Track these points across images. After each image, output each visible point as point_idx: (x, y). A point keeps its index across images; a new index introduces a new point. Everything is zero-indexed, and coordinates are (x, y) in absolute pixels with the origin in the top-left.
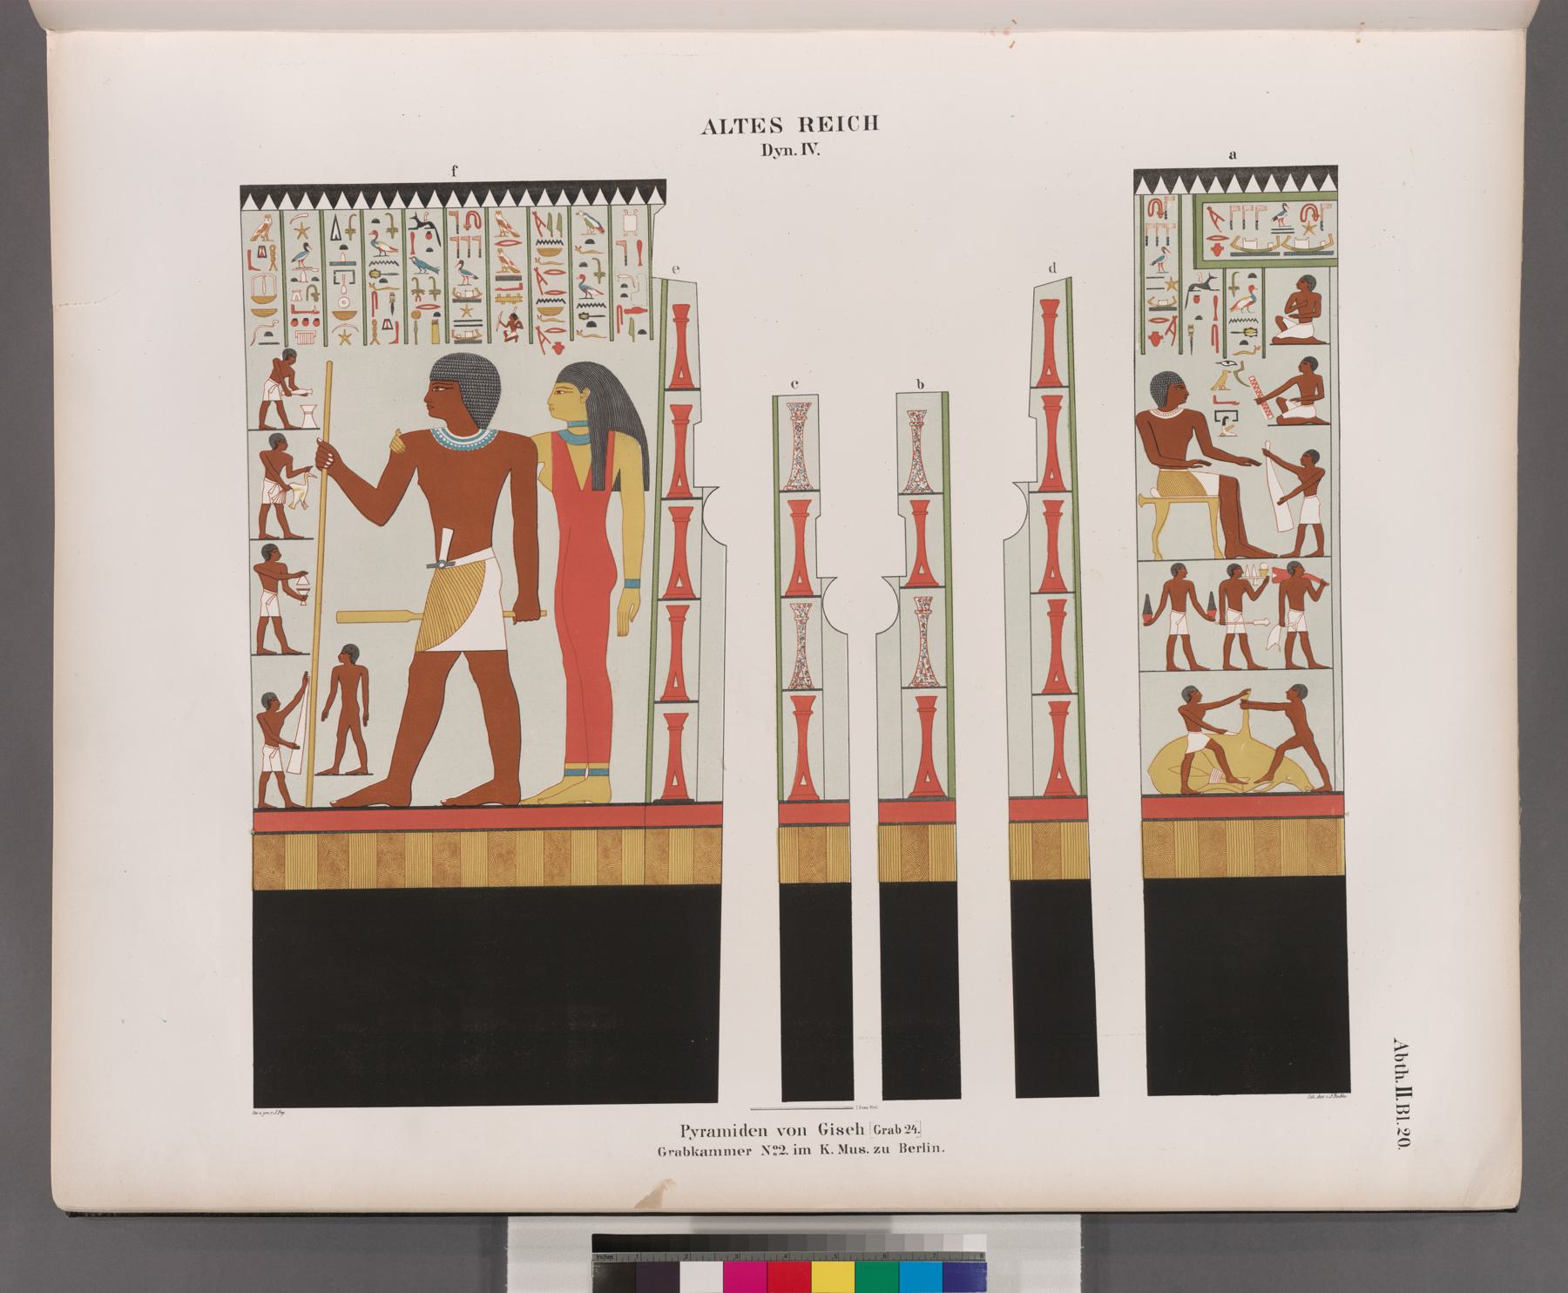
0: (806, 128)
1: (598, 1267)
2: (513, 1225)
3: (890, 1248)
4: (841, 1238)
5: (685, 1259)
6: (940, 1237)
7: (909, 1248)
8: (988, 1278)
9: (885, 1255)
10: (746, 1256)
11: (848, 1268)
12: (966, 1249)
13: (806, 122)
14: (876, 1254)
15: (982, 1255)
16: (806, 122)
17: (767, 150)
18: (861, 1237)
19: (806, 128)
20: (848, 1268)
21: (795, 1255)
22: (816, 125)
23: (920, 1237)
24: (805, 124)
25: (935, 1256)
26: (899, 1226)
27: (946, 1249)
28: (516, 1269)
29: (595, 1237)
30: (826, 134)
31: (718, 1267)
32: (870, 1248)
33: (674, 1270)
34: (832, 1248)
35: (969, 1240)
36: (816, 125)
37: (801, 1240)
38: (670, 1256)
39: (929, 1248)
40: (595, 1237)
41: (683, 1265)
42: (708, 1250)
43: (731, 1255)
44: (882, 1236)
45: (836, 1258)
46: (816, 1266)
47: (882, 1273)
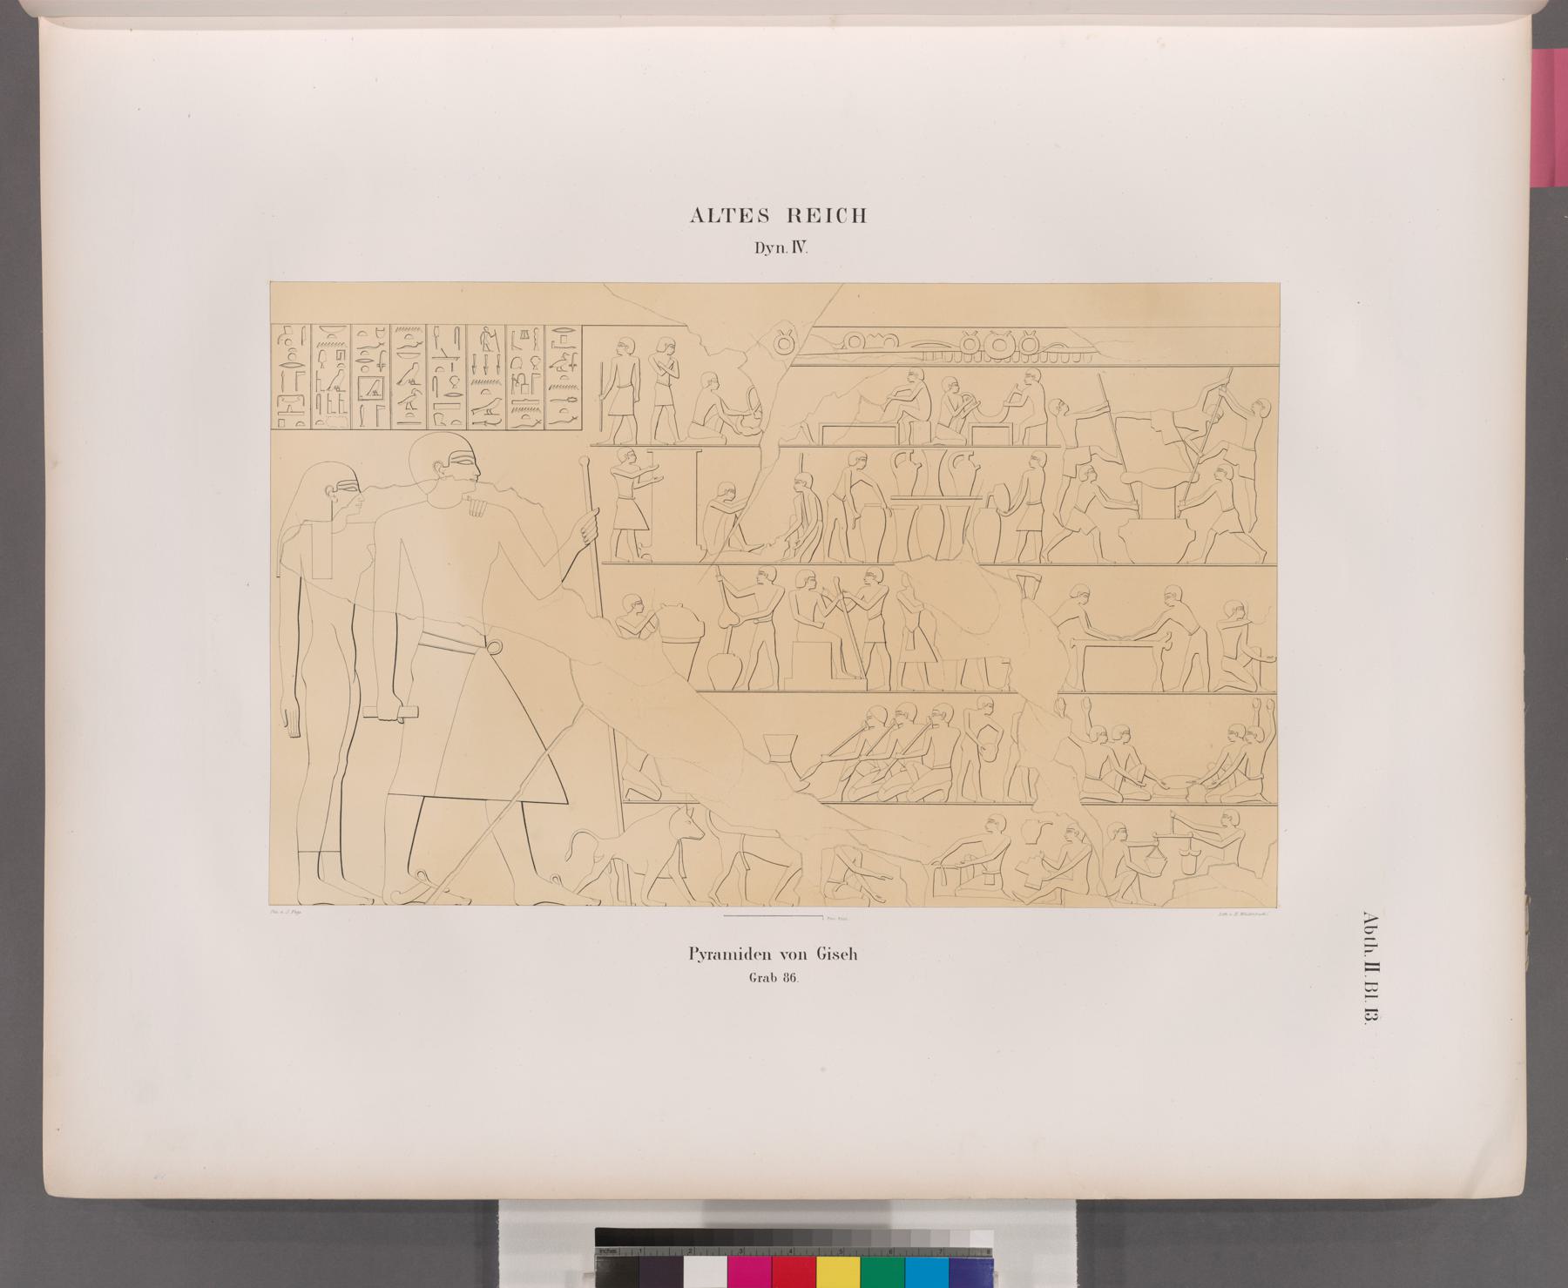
0: (794, 219)
1: (600, 1260)
5: (690, 1253)
6: (946, 1233)
7: (915, 1244)
9: (891, 1251)
10: (751, 1251)
11: (855, 1262)
13: (794, 212)
14: (882, 1250)
16: (794, 212)
17: (761, 248)
18: (866, 1233)
19: (794, 219)
20: (855, 1262)
21: (800, 1250)
22: (804, 216)
23: (926, 1233)
24: (793, 215)
25: (942, 1252)
27: (953, 1245)
29: (598, 1230)
30: (814, 224)
31: (724, 1259)
32: (875, 1245)
33: (678, 1264)
36: (804, 216)
38: (674, 1251)
39: (935, 1244)
40: (598, 1230)
43: (736, 1250)
44: (886, 1232)
45: (842, 1253)
46: (822, 1262)
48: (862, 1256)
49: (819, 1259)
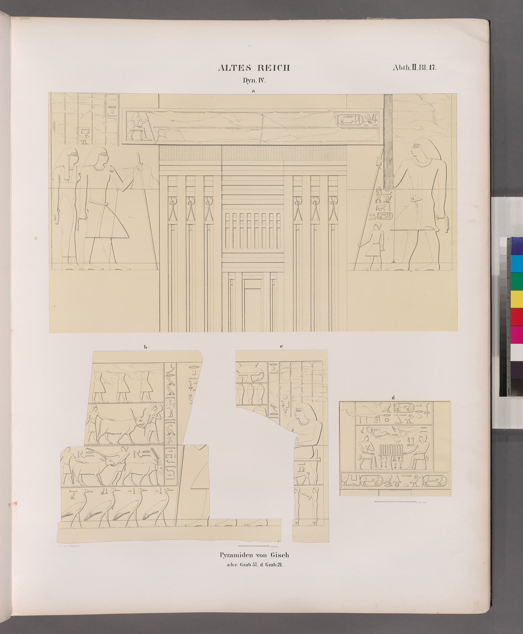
2: (496, 426)
3: (505, 276)
4: (501, 296)
5: (510, 359)
6: (501, 256)
7: (505, 268)
8: (518, 236)
10: (508, 334)
12: (506, 246)
14: (508, 282)
15: (508, 239)
18: (501, 288)
21: (508, 314)
23: (501, 264)
25: (508, 258)
26: (496, 272)
27: (506, 253)
28: (514, 426)
32: (505, 284)
33: (514, 363)
34: (505, 300)
35: (502, 245)
37: (502, 312)
38: (508, 365)
39: (505, 260)
41: (511, 360)
42: (506, 350)
43: (508, 340)
44: (500, 279)
45: (509, 298)
47: (515, 280)
48: (510, 290)
49: (512, 307)
